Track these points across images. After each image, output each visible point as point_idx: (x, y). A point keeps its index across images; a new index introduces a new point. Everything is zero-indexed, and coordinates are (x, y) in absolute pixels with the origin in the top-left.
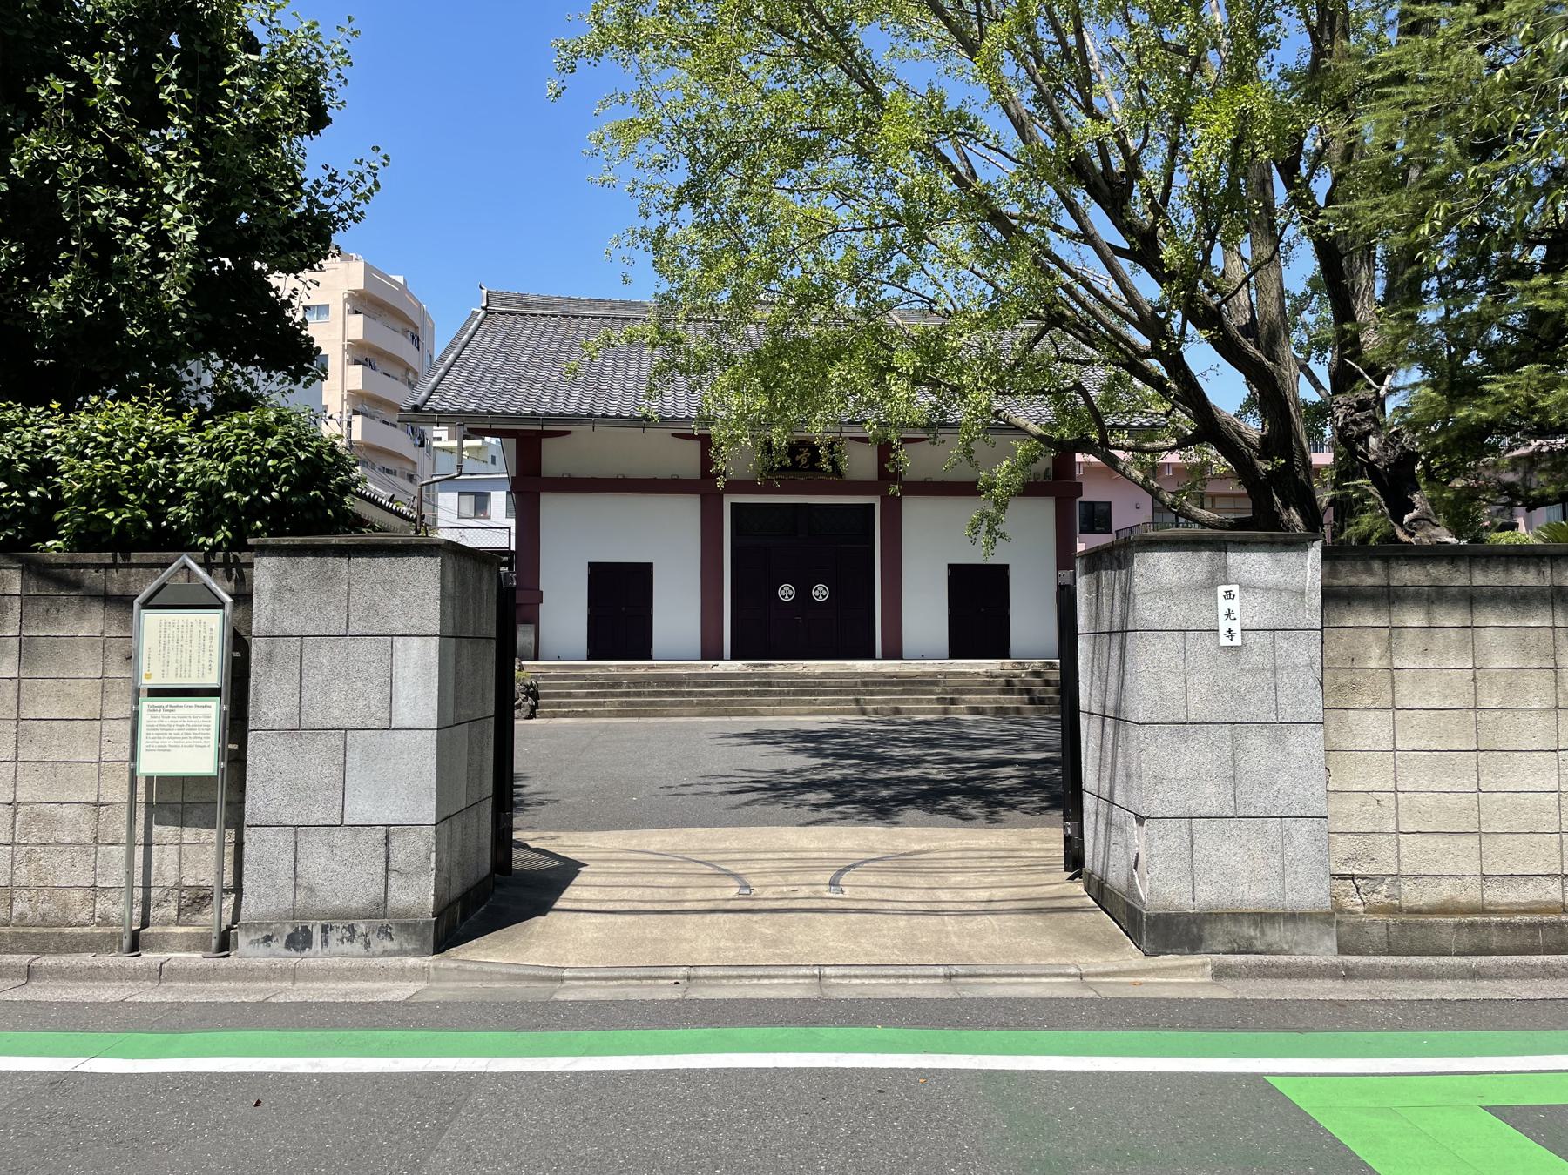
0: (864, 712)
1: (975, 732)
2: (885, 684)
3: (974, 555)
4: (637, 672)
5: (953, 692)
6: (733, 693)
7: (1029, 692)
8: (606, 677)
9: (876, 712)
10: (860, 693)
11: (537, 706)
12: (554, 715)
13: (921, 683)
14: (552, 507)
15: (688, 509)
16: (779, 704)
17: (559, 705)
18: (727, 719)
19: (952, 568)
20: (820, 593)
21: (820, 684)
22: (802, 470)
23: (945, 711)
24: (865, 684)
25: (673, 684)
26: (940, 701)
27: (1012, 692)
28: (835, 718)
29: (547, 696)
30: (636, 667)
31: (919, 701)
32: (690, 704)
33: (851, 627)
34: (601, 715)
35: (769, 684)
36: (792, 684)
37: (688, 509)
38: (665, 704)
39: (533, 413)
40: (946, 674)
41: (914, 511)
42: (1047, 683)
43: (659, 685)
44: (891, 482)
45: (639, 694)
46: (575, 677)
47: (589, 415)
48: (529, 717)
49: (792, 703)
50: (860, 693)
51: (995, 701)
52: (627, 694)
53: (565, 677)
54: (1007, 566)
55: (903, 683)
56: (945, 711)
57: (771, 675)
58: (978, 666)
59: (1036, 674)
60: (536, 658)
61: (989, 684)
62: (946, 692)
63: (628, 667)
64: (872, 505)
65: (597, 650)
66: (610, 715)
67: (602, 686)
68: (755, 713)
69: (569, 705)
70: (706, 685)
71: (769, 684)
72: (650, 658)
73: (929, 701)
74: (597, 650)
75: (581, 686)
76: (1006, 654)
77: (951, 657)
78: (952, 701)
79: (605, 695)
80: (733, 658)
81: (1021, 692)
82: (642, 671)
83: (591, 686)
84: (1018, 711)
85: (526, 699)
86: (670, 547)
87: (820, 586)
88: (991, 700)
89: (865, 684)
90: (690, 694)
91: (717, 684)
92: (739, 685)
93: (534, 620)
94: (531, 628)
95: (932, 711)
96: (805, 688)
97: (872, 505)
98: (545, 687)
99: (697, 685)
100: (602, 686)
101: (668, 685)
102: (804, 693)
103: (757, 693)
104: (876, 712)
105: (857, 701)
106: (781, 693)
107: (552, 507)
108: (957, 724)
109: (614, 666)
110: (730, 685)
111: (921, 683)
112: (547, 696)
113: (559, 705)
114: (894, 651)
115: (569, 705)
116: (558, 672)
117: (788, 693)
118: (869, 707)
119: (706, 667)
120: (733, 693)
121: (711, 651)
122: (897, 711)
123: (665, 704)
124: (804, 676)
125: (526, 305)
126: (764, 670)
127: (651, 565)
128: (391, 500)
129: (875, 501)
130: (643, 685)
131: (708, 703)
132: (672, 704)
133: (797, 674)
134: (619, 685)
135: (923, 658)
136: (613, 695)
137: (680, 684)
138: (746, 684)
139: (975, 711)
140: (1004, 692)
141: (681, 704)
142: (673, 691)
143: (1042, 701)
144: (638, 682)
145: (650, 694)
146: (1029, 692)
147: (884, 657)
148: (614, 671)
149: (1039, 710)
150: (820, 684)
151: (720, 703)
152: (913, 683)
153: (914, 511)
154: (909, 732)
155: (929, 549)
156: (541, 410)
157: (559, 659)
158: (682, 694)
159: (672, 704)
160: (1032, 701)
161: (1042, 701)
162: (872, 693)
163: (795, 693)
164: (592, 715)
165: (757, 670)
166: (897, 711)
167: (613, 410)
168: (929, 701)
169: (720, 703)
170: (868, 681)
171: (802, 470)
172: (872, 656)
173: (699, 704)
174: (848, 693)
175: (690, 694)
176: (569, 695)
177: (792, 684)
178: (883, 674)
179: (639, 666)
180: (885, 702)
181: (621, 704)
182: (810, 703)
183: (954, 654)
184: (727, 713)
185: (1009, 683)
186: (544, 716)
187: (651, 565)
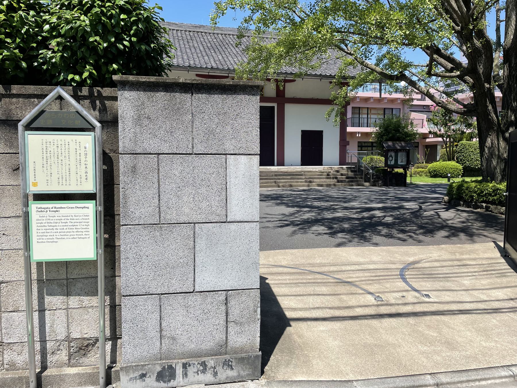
0: (279, 187)
2: (284, 175)
7: (336, 178)
9: (283, 186)
13: (297, 175)
19: (302, 131)
24: (276, 175)
27: (330, 178)
31: (297, 182)
41: (290, 109)
42: (342, 175)
51: (325, 182)
54: (322, 132)
55: (290, 175)
56: (308, 186)
58: (316, 168)
59: (338, 171)
61: (321, 175)
62: (306, 178)
73: (301, 182)
76: (321, 164)
77: (302, 165)
78: (310, 182)
84: (335, 185)
88: (325, 181)
89: (276, 175)
95: (303, 186)
104: (283, 186)
105: (275, 182)
111: (297, 175)
114: (281, 163)
118: (281, 184)
122: (291, 186)
129: (275, 105)
135: (292, 165)
139: (319, 185)
140: (327, 178)
143: (342, 181)
146: (336, 178)
147: (278, 165)
152: (293, 175)
153: (290, 109)
160: (338, 182)
161: (342, 181)
162: (279, 179)
168: (301, 182)
172: (273, 165)
174: (270, 179)
178: (282, 172)
185: (328, 175)
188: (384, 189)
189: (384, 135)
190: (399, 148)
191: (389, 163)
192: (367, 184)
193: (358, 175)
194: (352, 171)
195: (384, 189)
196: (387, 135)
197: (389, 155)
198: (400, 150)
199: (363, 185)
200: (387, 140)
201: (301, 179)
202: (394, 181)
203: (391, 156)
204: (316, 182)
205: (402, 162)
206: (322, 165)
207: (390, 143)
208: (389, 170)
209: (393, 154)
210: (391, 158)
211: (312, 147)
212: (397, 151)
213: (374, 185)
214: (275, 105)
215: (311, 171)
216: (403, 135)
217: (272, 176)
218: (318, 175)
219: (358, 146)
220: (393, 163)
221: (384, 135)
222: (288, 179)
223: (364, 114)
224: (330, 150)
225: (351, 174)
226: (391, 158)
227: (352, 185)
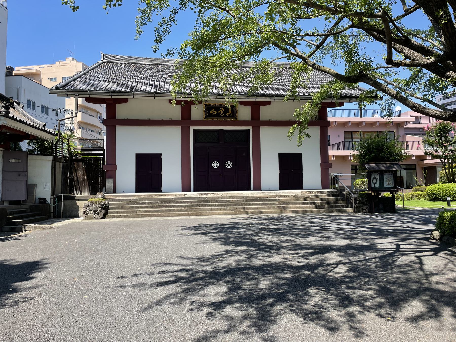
0: (247, 213)
1: (300, 224)
2: (255, 201)
3: (291, 148)
4: (153, 197)
5: (283, 204)
6: (192, 206)
7: (314, 203)
8: (140, 200)
9: (252, 213)
10: (245, 205)
11: (107, 213)
12: (114, 217)
13: (270, 200)
14: (120, 131)
15: (176, 132)
16: (211, 210)
17: (117, 213)
18: (188, 217)
20: (229, 165)
21: (229, 201)
22: (221, 116)
23: (281, 212)
24: (247, 201)
25: (167, 203)
26: (279, 207)
27: (307, 204)
28: (235, 216)
29: (113, 208)
30: (152, 195)
31: (269, 208)
32: (174, 211)
33: (241, 178)
34: (134, 217)
35: (208, 202)
36: (217, 202)
37: (176, 132)
38: (163, 211)
39: (107, 90)
40: (280, 196)
41: (266, 133)
43: (161, 203)
44: (256, 121)
45: (152, 207)
46: (127, 200)
47: (131, 91)
48: (102, 218)
49: (217, 209)
50: (245, 205)
52: (147, 207)
53: (122, 200)
54: (301, 154)
55: (262, 200)
56: (281, 212)
57: (208, 198)
60: (114, 192)
61: (297, 200)
62: (280, 204)
63: (149, 196)
64: (248, 131)
65: (139, 189)
66: (138, 216)
67: (137, 204)
68: (201, 214)
69: (121, 212)
70: (181, 203)
71: (208, 202)
72: (161, 191)
73: (274, 208)
74: (139, 189)
75: (128, 204)
76: (302, 188)
77: (280, 189)
78: (284, 208)
79: (138, 208)
80: (195, 190)
81: (311, 203)
82: (155, 197)
83: (132, 204)
84: (312, 211)
85: (101, 210)
86: (169, 147)
87: (229, 162)
88: (300, 207)
89: (247, 201)
90: (174, 206)
91: (186, 202)
92: (195, 202)
93: (113, 177)
94: (112, 180)
95: (275, 212)
96: (222, 203)
97: (248, 131)
98: (113, 204)
99: (177, 203)
100: (137, 204)
101: (165, 203)
102: (222, 205)
103: (202, 206)
104: (252, 213)
105: (244, 208)
106: (212, 206)
107: (120, 131)
108: (288, 219)
109: (143, 195)
110: (191, 202)
111: (270, 200)
112: (113, 208)
113: (117, 213)
114: (258, 187)
115: (121, 212)
116: (120, 198)
117: (215, 206)
118: (249, 211)
119: (182, 195)
120: (192, 206)
121: (186, 188)
122: (261, 212)
123: (163, 211)
124: (222, 198)
125: (118, 59)
126: (206, 196)
127: (161, 155)
128: (44, 126)
129: (250, 128)
130: (154, 203)
131: (181, 210)
132: (166, 211)
133: (219, 198)
134: (145, 203)
135: (269, 190)
136: (141, 208)
137: (170, 202)
138: (198, 202)
139: (293, 212)
141: (170, 211)
142: (168, 205)
144: (153, 202)
145: (157, 207)
146: (314, 203)
147: (255, 189)
148: (143, 197)
149: (319, 211)
150: (229, 201)
151: (186, 210)
152: (266, 200)
153: (265, 132)
154: (268, 225)
155: (271, 146)
156: (111, 89)
157: (124, 192)
158: (171, 207)
159: (166, 211)
160: (316, 207)
162: (250, 205)
163: (218, 205)
164: (131, 217)
165: (203, 196)
166: (261, 212)
167: (142, 89)
168: (274, 208)
169: (186, 210)
170: (249, 200)
171: (221, 116)
172: (249, 189)
173: (177, 211)
174: (240, 205)
175: (174, 206)
176: (122, 208)
177: (217, 202)
178: (254, 197)
179: (154, 195)
180: (255, 208)
181: (144, 212)
182: (224, 209)
183: (281, 188)
184: (189, 215)
185: (305, 200)
186: (110, 217)
187: (161, 155)
188: (367, 216)
189: (365, 155)
190: (383, 168)
191: (373, 186)
192: (350, 210)
193: (339, 199)
194: (333, 196)
195: (367, 216)
196: (369, 155)
197: (373, 176)
198: (386, 172)
199: (345, 212)
200: (370, 161)
201: (274, 204)
202: (381, 207)
203: (375, 178)
204: (290, 208)
205: (388, 184)
206: (302, 189)
207: (373, 164)
208: (373, 194)
209: (377, 177)
210: (375, 181)
211: (291, 171)
212: (381, 173)
213: (357, 211)
214: (250, 128)
215: (286, 196)
216: (388, 154)
217: (243, 202)
218: (295, 200)
219: (352, 170)
220: (377, 186)
221: (365, 155)
222: (259, 205)
223: (357, 138)
224: (311, 173)
225: (332, 199)
226: (375, 181)
227: (332, 212)
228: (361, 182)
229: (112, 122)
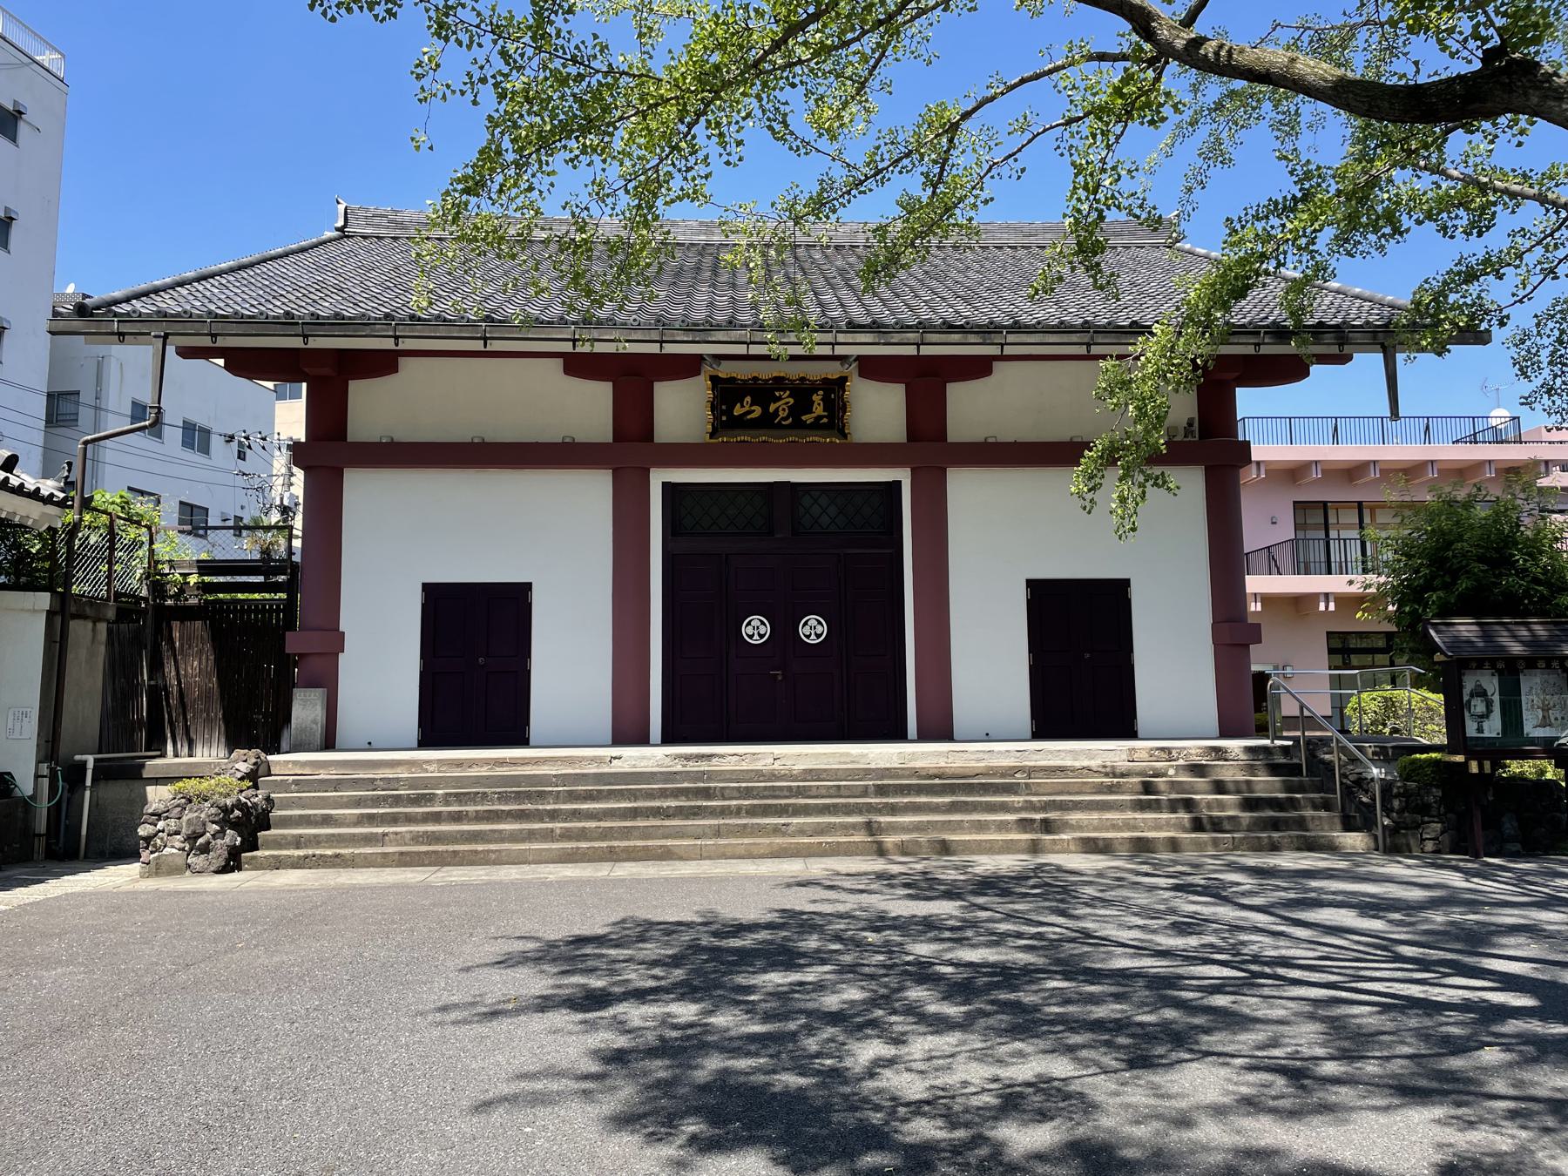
0: (881, 852)
2: (920, 790)
3: (1080, 559)
5: (1046, 807)
6: (634, 813)
7: (1189, 805)
8: (413, 783)
9: (904, 849)
10: (878, 810)
12: (278, 864)
14: (363, 491)
15: (592, 492)
16: (718, 832)
17: (298, 843)
19: (1032, 584)
20: (813, 629)
21: (800, 792)
22: (780, 426)
24: (881, 791)
25: (528, 796)
26: (1024, 825)
27: (1154, 806)
28: (817, 868)
29: (286, 822)
30: (472, 763)
31: (981, 827)
32: (548, 836)
33: (863, 690)
35: (707, 793)
36: (747, 793)
37: (592, 492)
38: (501, 837)
40: (1030, 771)
41: (971, 495)
42: (1220, 787)
43: (503, 798)
44: (930, 446)
45: (457, 818)
46: (356, 784)
49: (743, 831)
50: (870, 809)
51: (1128, 826)
52: (436, 818)
53: (337, 785)
56: (1035, 848)
57: (711, 776)
58: (1090, 754)
59: (1197, 770)
60: (329, 744)
61: (1111, 789)
62: (1031, 807)
63: (459, 764)
64: (897, 485)
66: (385, 861)
67: (397, 800)
68: (667, 855)
69: (316, 841)
71: (707, 793)
75: (358, 802)
78: (1047, 826)
79: (394, 820)
80: (668, 739)
81: (1173, 806)
82: (484, 772)
83: (376, 801)
84: (1174, 845)
86: (562, 551)
87: (812, 619)
89: (881, 791)
90: (554, 815)
91: (610, 795)
92: (650, 795)
93: (327, 682)
95: (1008, 848)
96: (770, 799)
97: (897, 485)
99: (573, 797)
100: (397, 800)
101: (519, 797)
102: (766, 811)
103: (680, 812)
104: (904, 849)
105: (870, 828)
106: (723, 812)
107: (363, 491)
110: (634, 795)
112: (286, 822)
113: (298, 843)
114: (939, 728)
117: (738, 812)
118: (890, 840)
120: (634, 813)
121: (629, 731)
122: (945, 848)
123: (501, 837)
124: (774, 776)
125: (401, 225)
126: (704, 766)
127: (526, 588)
129: (903, 476)
131: (582, 835)
132: (514, 837)
133: (759, 775)
134: (430, 799)
135: (988, 738)
136: (410, 819)
137: (541, 796)
138: (663, 794)
140: (1141, 806)
141: (531, 836)
143: (1217, 825)
145: (480, 817)
146: (1189, 805)
147: (923, 737)
150: (800, 792)
151: (606, 834)
152: (970, 789)
154: (959, 933)
155: (995, 549)
157: (370, 747)
158: (539, 816)
159: (514, 837)
160: (1198, 825)
161: (1217, 825)
162: (893, 810)
163: (752, 812)
165: (692, 767)
166: (945, 848)
168: (1002, 826)
169: (606, 834)
170: (889, 786)
171: (780, 426)
172: (899, 735)
173: (567, 835)
174: (849, 810)
175: (554, 815)
176: (327, 821)
177: (747, 793)
178: (915, 773)
180: (918, 827)
181: (417, 839)
182: (776, 830)
185: (1148, 788)
186: (258, 866)
187: (526, 588)
188: (1456, 880)
189: (1428, 586)
190: (1516, 649)
191: (1471, 729)
192: (1355, 840)
193: (1307, 787)
194: (1274, 769)
195: (1456, 880)
196: (1447, 587)
197: (1469, 684)
198: (1530, 663)
199: (1331, 848)
200: (1447, 611)
201: (1004, 808)
202: (1509, 826)
203: (1482, 693)
204: (1080, 828)
205: (1545, 723)
206: (1133, 735)
207: (1466, 628)
208: (1474, 767)
209: (1492, 684)
210: (1479, 706)
211: (1080, 657)
212: (1510, 670)
213: (1393, 846)
214: (903, 476)
215: (1062, 769)
216: (1536, 581)
217: (865, 792)
218: (1101, 789)
219: (1331, 651)
220: (1493, 728)
221: (1428, 586)
222: (935, 809)
223: (1348, 527)
224: (1172, 666)
225: (1266, 784)
226: (1479, 706)
227: (1274, 848)
228: (1421, 713)
229: (328, 453)
